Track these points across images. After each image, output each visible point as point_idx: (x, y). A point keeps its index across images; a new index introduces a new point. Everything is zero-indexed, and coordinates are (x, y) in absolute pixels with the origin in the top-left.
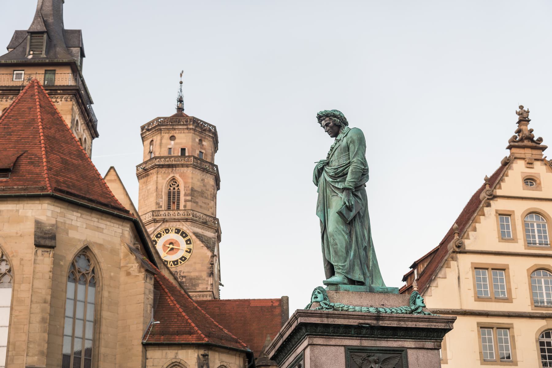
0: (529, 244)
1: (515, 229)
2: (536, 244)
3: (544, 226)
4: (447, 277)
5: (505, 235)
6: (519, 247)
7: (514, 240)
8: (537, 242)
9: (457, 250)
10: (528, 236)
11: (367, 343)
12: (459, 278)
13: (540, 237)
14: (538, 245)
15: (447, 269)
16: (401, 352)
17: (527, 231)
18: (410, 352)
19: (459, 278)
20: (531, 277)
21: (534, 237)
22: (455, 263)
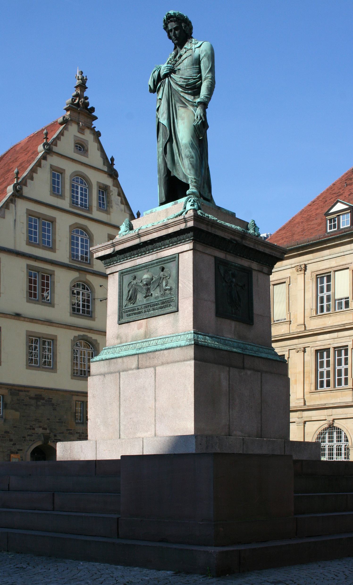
0: (74, 203)
1: (63, 187)
2: (78, 205)
3: (86, 191)
4: (6, 217)
5: (56, 190)
6: (65, 204)
7: (61, 196)
8: (79, 203)
9: (17, 194)
10: (73, 196)
11: (230, 258)
12: (15, 220)
13: (82, 199)
14: (79, 206)
15: (6, 210)
16: (248, 272)
17: (73, 191)
18: (254, 273)
19: (15, 220)
20: (71, 231)
21: (77, 198)
22: (13, 205)
